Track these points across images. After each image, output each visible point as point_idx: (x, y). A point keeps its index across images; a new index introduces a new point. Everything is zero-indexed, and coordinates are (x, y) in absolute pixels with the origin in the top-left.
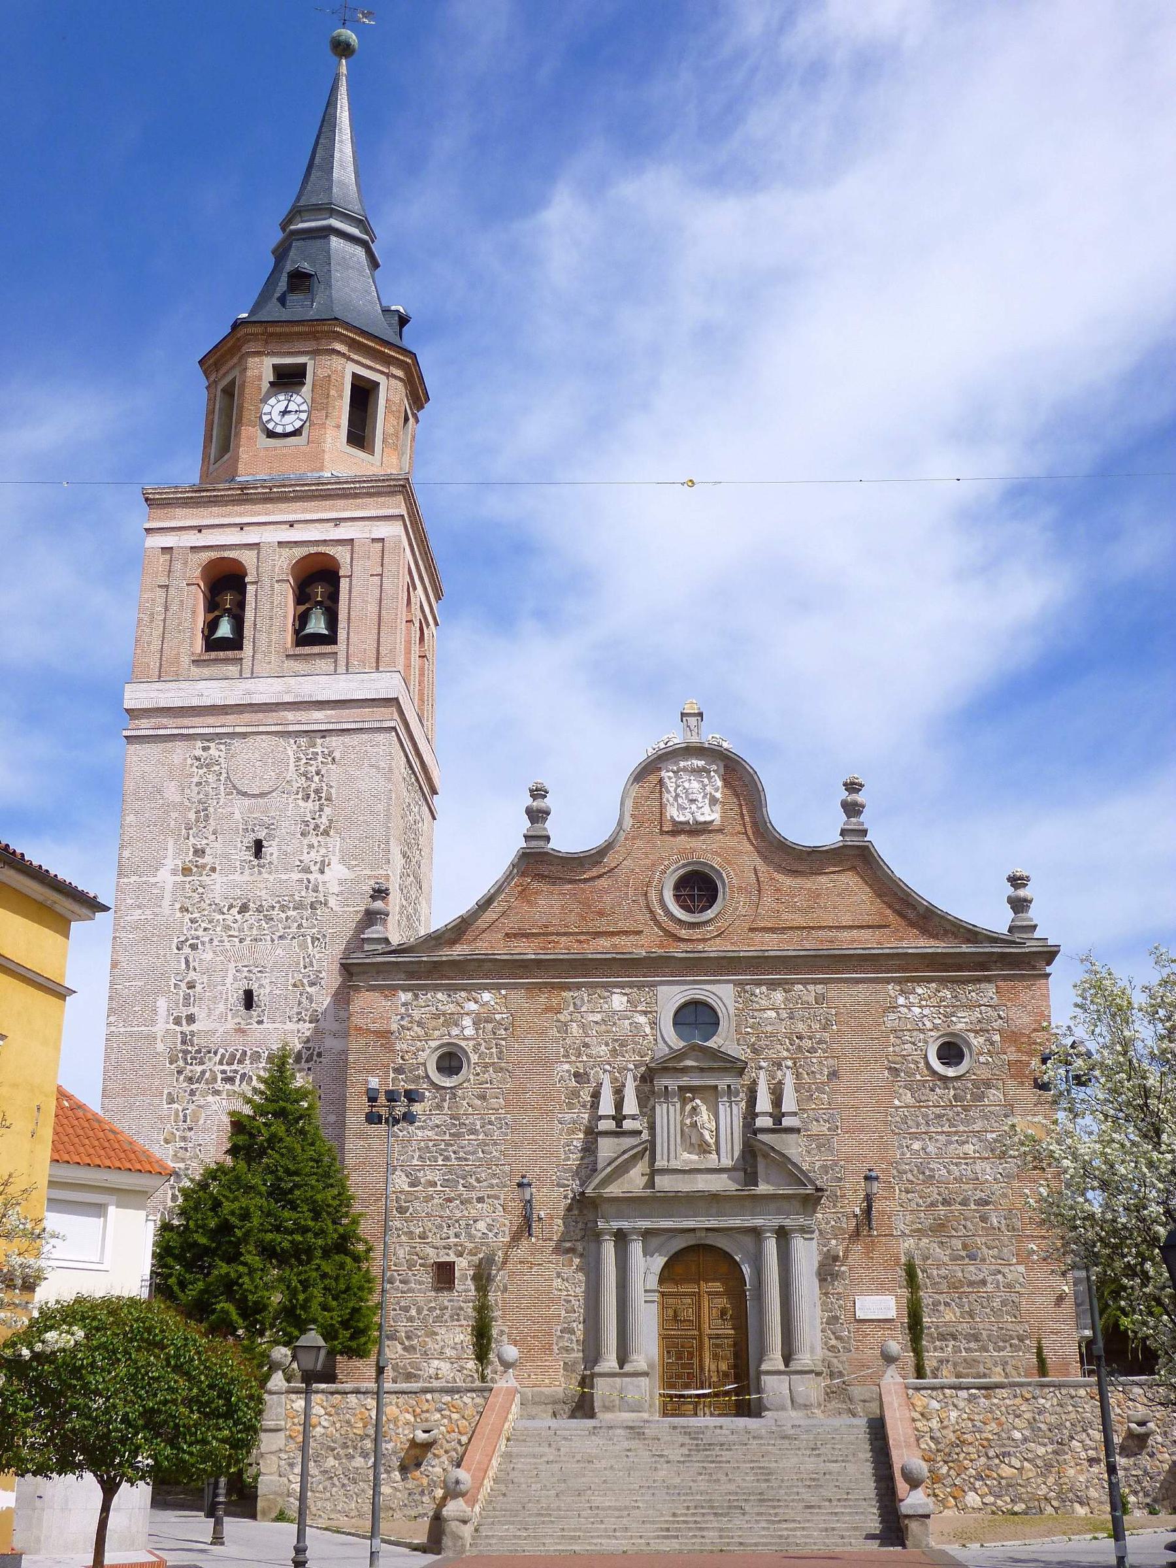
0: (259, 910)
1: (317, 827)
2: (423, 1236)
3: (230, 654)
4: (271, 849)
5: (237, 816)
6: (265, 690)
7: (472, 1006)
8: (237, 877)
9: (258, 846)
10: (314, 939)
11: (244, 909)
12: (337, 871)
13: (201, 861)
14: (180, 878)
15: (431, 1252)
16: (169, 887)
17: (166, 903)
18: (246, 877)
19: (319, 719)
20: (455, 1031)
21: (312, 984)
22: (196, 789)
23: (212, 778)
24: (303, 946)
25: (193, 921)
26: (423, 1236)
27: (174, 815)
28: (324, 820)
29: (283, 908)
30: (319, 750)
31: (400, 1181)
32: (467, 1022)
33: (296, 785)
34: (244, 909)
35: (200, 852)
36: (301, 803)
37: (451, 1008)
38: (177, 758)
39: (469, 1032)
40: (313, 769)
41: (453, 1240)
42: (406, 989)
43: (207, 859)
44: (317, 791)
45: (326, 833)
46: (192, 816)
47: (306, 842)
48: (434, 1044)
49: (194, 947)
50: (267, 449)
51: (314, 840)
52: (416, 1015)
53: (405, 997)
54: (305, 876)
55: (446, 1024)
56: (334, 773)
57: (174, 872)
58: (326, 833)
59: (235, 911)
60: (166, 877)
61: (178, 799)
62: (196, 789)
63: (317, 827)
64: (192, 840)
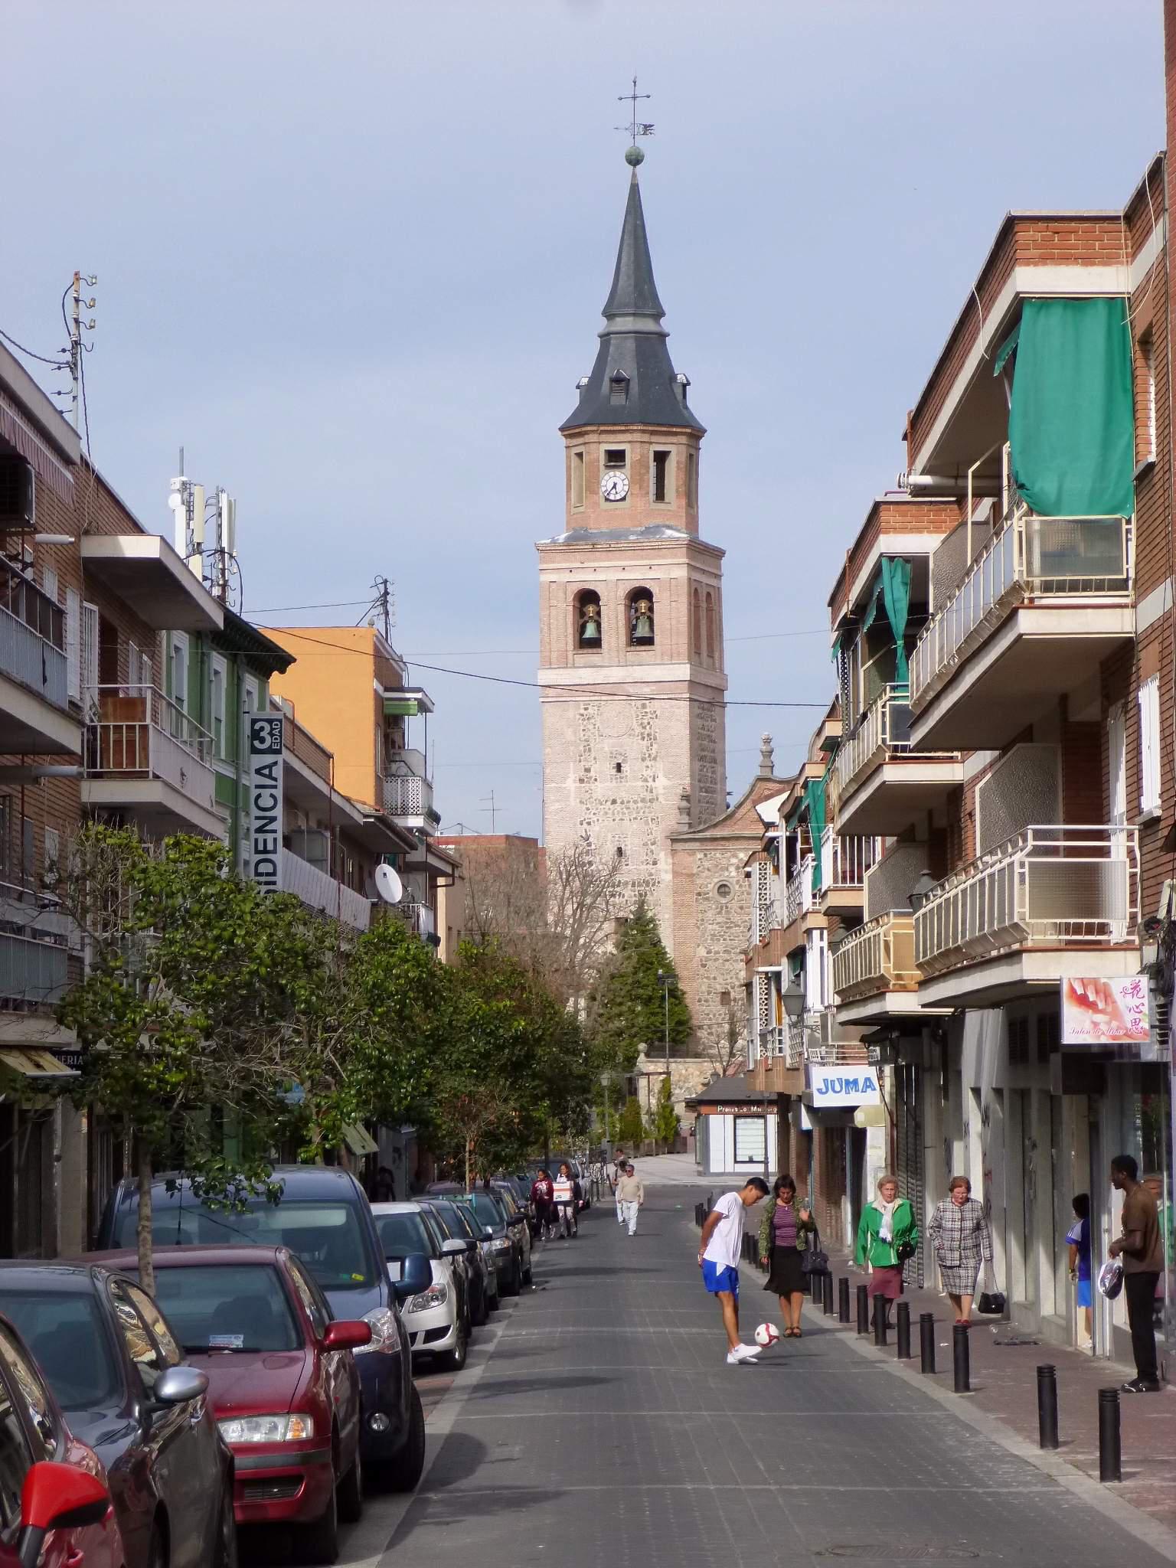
0: (622, 803)
1: (650, 755)
2: (715, 978)
3: (595, 650)
4: (625, 768)
5: (606, 749)
6: (616, 674)
7: (734, 861)
8: (608, 784)
9: (619, 767)
10: (652, 819)
11: (614, 802)
12: (662, 782)
13: (589, 775)
14: (578, 785)
15: (718, 986)
16: (573, 789)
17: (572, 799)
18: (614, 783)
19: (646, 690)
20: (726, 874)
21: (652, 844)
22: (582, 733)
23: (591, 727)
24: (647, 823)
25: (588, 809)
26: (715, 978)
27: (572, 748)
28: (654, 751)
29: (635, 802)
30: (647, 710)
31: (702, 952)
32: (732, 869)
33: (637, 732)
34: (614, 802)
35: (588, 770)
36: (640, 742)
37: (724, 862)
38: (571, 714)
39: (734, 874)
40: (646, 721)
41: (729, 981)
42: (701, 850)
43: (592, 774)
44: (648, 735)
45: (655, 759)
46: (582, 748)
47: (645, 764)
48: (716, 880)
49: (589, 823)
50: (606, 511)
51: (649, 763)
52: (707, 864)
53: (700, 855)
54: (645, 784)
55: (722, 869)
56: (655, 723)
57: (575, 781)
58: (655, 759)
59: (609, 803)
60: (571, 784)
61: (573, 739)
62: (582, 733)
63: (650, 755)
64: (582, 763)
